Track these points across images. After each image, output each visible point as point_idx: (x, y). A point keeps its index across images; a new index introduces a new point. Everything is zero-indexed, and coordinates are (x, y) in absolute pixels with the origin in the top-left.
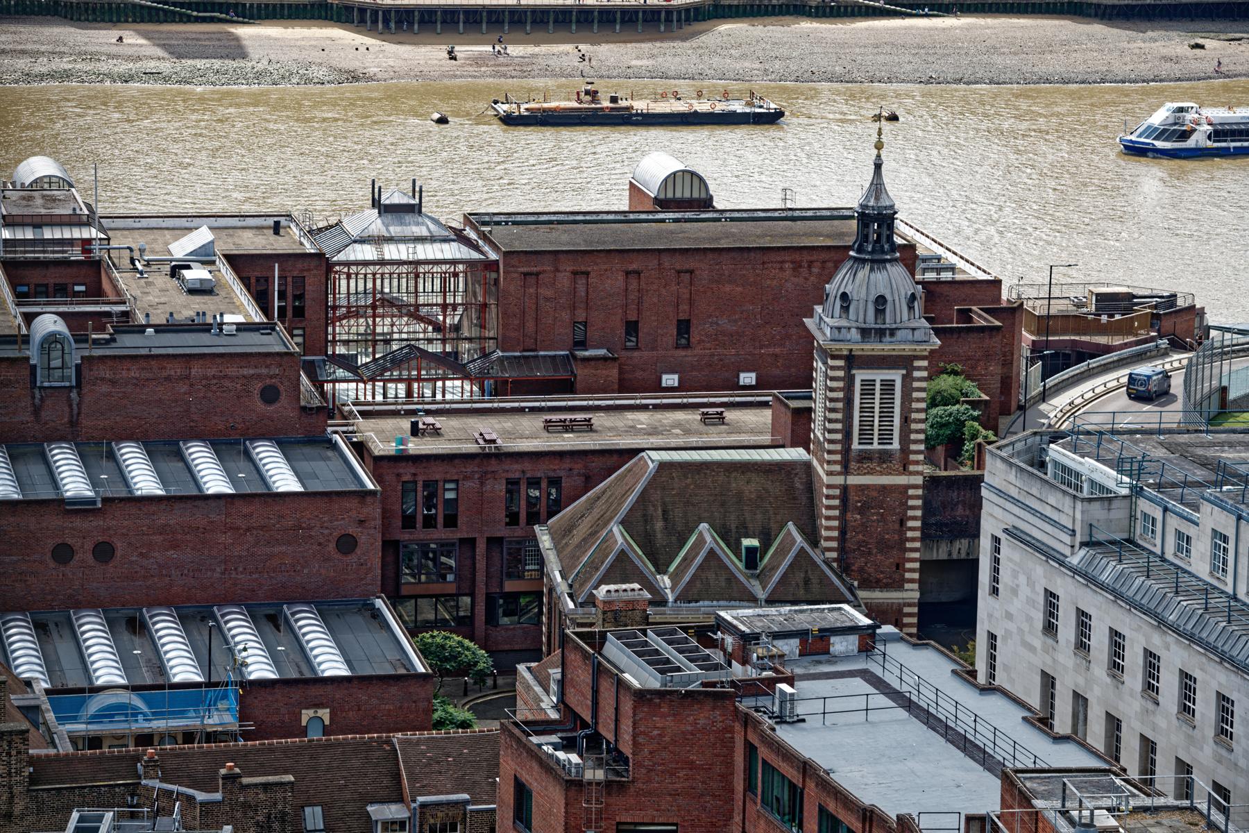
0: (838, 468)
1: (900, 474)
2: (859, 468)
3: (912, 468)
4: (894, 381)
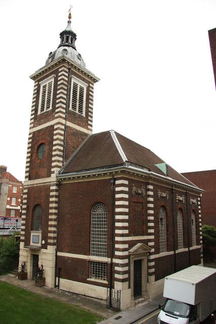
3: (89, 127)
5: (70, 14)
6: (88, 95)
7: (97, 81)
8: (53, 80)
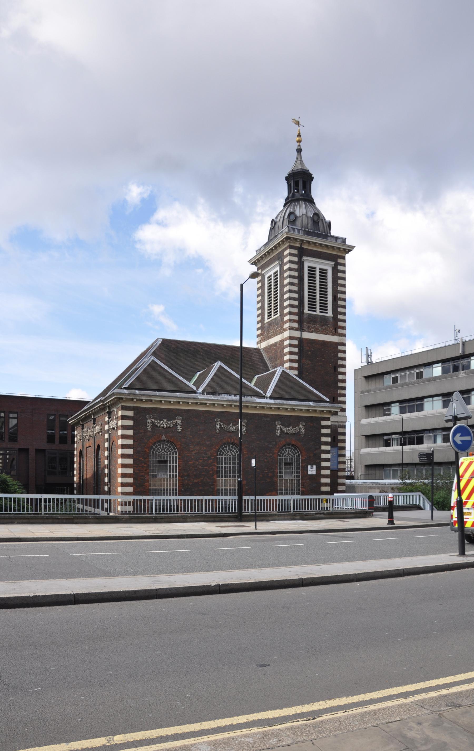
0: (296, 325)
1: (333, 335)
2: (309, 327)
3: (340, 331)
4: (326, 270)
5: (299, 135)
6: (335, 279)
7: (350, 251)
8: (278, 269)
